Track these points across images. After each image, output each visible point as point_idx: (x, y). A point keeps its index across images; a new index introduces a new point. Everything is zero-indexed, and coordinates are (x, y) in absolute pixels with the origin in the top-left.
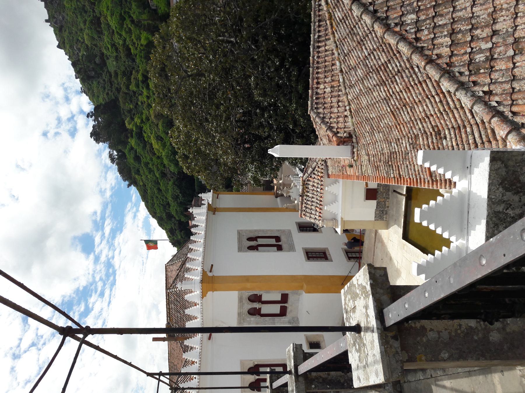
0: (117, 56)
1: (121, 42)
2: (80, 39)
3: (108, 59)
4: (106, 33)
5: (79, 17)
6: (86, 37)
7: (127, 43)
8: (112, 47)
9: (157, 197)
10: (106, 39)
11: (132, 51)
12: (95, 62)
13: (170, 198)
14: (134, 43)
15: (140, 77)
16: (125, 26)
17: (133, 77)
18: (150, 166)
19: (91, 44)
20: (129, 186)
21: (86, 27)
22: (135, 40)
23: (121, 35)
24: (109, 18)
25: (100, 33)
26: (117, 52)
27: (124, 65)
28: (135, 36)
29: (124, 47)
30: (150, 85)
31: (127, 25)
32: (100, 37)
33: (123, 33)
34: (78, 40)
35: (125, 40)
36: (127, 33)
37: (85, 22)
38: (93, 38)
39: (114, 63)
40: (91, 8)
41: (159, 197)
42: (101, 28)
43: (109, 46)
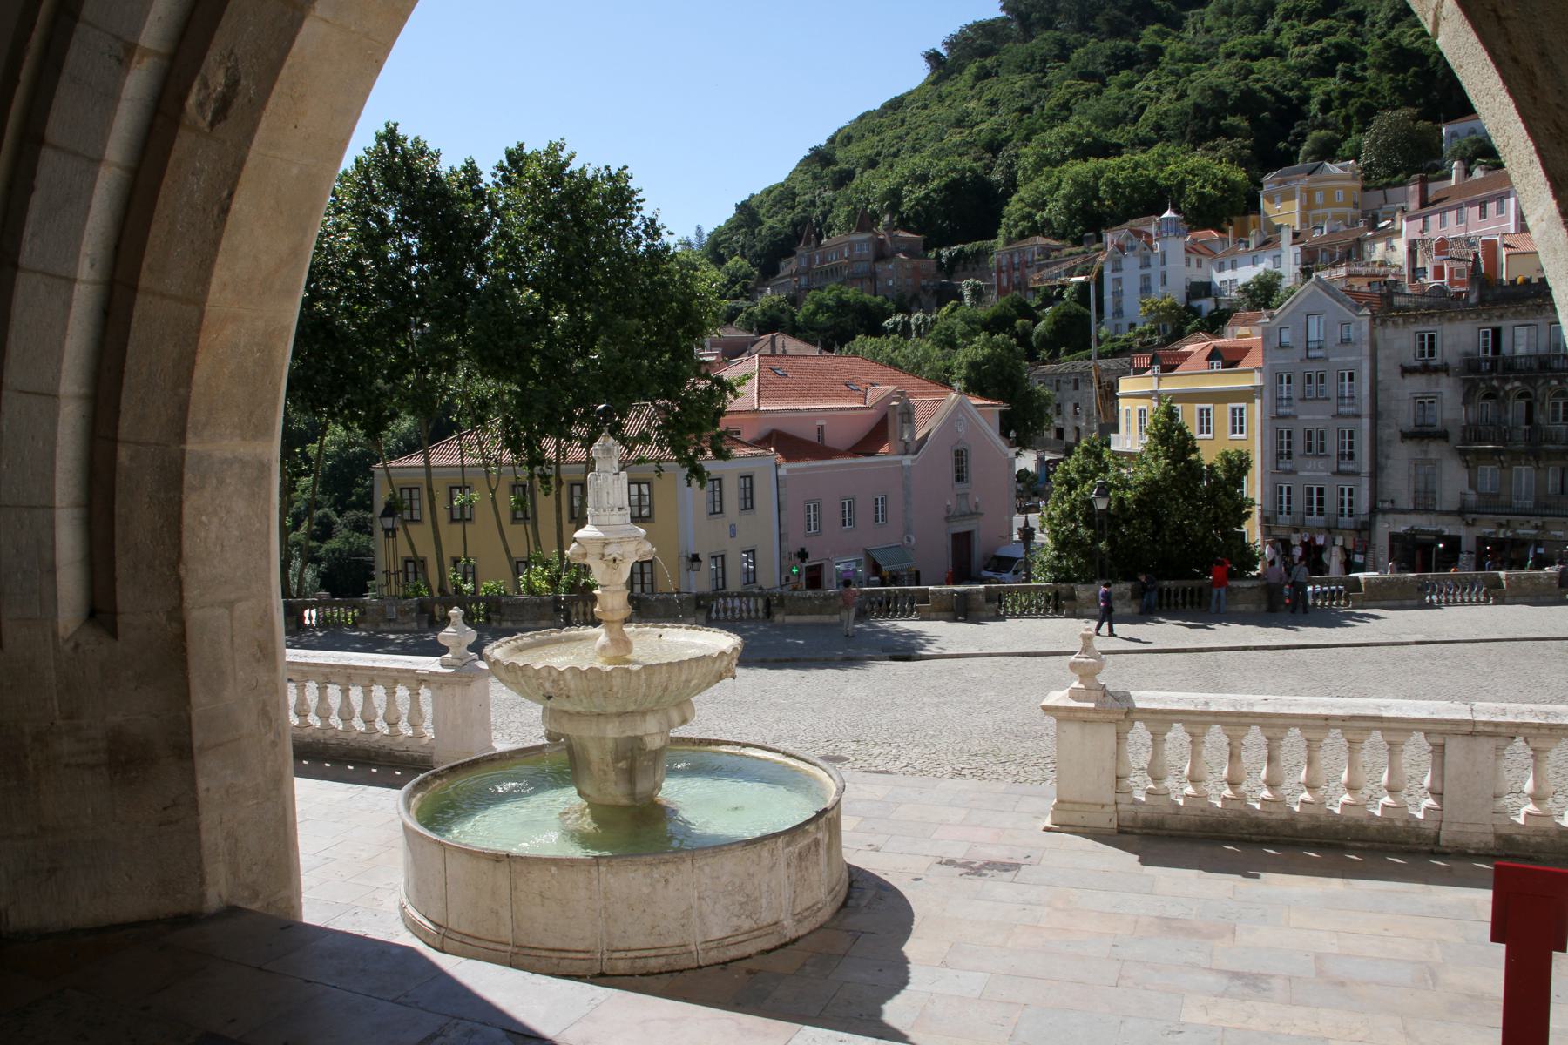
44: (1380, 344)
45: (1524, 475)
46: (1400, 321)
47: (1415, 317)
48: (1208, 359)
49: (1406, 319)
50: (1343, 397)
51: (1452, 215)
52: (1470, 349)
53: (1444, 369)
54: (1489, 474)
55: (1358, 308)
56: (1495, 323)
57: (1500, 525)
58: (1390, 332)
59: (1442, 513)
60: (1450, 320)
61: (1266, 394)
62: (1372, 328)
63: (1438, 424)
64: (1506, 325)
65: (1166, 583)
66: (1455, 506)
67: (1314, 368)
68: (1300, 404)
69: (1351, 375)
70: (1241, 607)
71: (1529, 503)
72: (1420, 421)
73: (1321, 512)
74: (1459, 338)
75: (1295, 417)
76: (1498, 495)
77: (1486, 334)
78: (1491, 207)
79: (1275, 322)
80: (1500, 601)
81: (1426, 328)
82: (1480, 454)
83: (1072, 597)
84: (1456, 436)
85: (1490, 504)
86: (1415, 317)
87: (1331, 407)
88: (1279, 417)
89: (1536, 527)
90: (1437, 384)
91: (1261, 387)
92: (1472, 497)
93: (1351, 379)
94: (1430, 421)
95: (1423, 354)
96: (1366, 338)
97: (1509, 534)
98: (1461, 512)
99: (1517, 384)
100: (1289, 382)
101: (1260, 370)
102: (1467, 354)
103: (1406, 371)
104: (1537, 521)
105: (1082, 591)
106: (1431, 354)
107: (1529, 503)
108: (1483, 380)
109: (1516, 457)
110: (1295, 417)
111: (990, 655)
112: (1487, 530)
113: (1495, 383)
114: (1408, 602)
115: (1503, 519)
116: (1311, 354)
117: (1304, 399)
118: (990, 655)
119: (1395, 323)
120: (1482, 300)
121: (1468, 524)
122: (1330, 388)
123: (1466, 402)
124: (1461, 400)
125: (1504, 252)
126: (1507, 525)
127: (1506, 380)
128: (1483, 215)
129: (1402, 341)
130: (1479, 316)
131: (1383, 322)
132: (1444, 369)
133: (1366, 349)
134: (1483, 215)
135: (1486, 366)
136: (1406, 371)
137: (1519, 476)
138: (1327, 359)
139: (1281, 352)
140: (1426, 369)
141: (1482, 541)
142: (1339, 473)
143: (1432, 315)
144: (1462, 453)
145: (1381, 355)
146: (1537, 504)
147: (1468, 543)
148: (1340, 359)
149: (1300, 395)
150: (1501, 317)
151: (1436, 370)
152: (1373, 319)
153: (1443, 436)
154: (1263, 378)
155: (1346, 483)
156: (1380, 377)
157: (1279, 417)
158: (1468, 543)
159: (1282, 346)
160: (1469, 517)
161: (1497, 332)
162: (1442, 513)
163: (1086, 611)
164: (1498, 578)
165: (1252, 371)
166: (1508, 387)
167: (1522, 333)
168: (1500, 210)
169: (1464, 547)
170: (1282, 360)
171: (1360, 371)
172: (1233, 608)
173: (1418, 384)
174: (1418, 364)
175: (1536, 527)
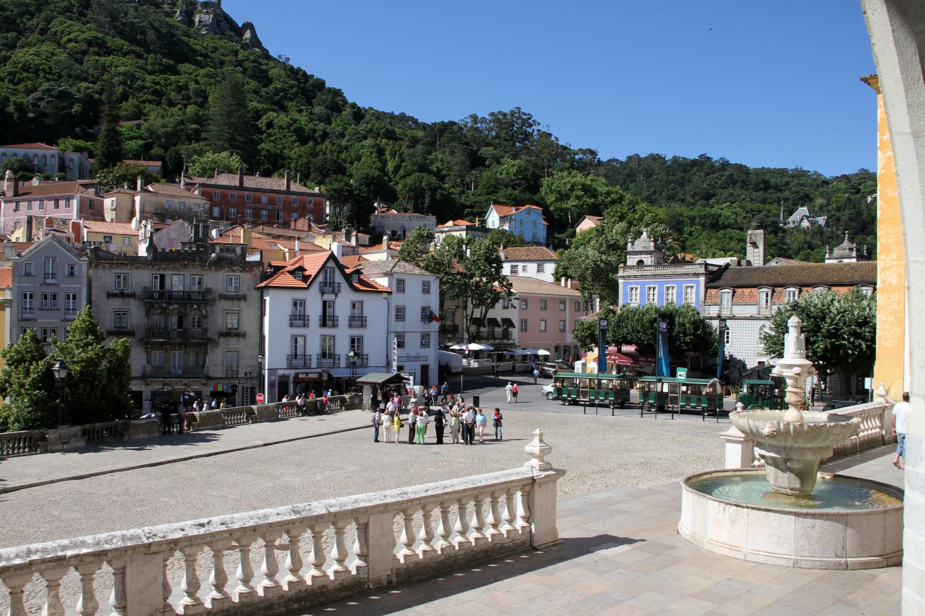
44: (94, 279)
45: (177, 357)
46: (107, 266)
47: (116, 264)
49: (111, 265)
50: (69, 309)
51: (36, 204)
52: (148, 285)
54: (157, 355)
55: (80, 256)
56: (162, 272)
57: (166, 384)
58: (100, 272)
60: (137, 268)
61: (15, 305)
62: (88, 268)
63: (129, 327)
64: (168, 273)
65: (97, 424)
66: (139, 374)
67: (50, 291)
68: (40, 312)
70: (141, 436)
71: (180, 372)
72: (117, 325)
74: (141, 279)
75: (36, 320)
76: (163, 367)
77: (156, 278)
78: (62, 203)
79: (23, 259)
80: (255, 422)
81: (123, 271)
82: (154, 344)
83: (43, 438)
84: (140, 334)
85: (159, 372)
86: (116, 264)
87: (61, 315)
88: (24, 320)
89: (185, 384)
90: (128, 304)
91: (11, 301)
92: (149, 369)
94: (124, 325)
95: (119, 286)
96: (84, 274)
97: (170, 388)
98: (144, 377)
99: (176, 306)
100: (31, 297)
101: (11, 289)
102: (145, 288)
103: (110, 295)
104: (185, 381)
105: (51, 434)
106: (125, 285)
107: (180, 372)
108: (157, 303)
109: (173, 346)
110: (36, 320)
111: (52, 482)
112: (157, 387)
113: (164, 305)
114: (218, 426)
115: (168, 380)
116: (48, 281)
117: (42, 309)
118: (52, 482)
119: (104, 268)
120: (155, 259)
121: (147, 384)
122: (61, 302)
123: (147, 316)
124: (144, 313)
125: (85, 231)
126: (169, 385)
127: (170, 304)
128: (57, 206)
129: (107, 278)
130: (153, 267)
131: (97, 266)
132: (133, 295)
133: (85, 281)
134: (57, 206)
135: (156, 295)
136: (110, 295)
137: (174, 357)
138: (58, 285)
139: (26, 279)
140: (122, 295)
141: (154, 394)
143: (127, 265)
144: (146, 344)
145: (93, 285)
146: (183, 372)
147: (146, 395)
148: (68, 286)
149: (39, 306)
150: (165, 269)
151: (129, 296)
152: (90, 264)
153: (131, 334)
154: (12, 295)
157: (24, 320)
158: (146, 395)
159: (28, 275)
160: (149, 380)
161: (162, 277)
163: (54, 448)
164: (252, 410)
165: (4, 290)
166: (171, 308)
167: (175, 278)
168: (68, 205)
169: (144, 397)
170: (28, 285)
171: (80, 294)
172: (137, 437)
173: (117, 303)
174: (117, 291)
175: (185, 384)
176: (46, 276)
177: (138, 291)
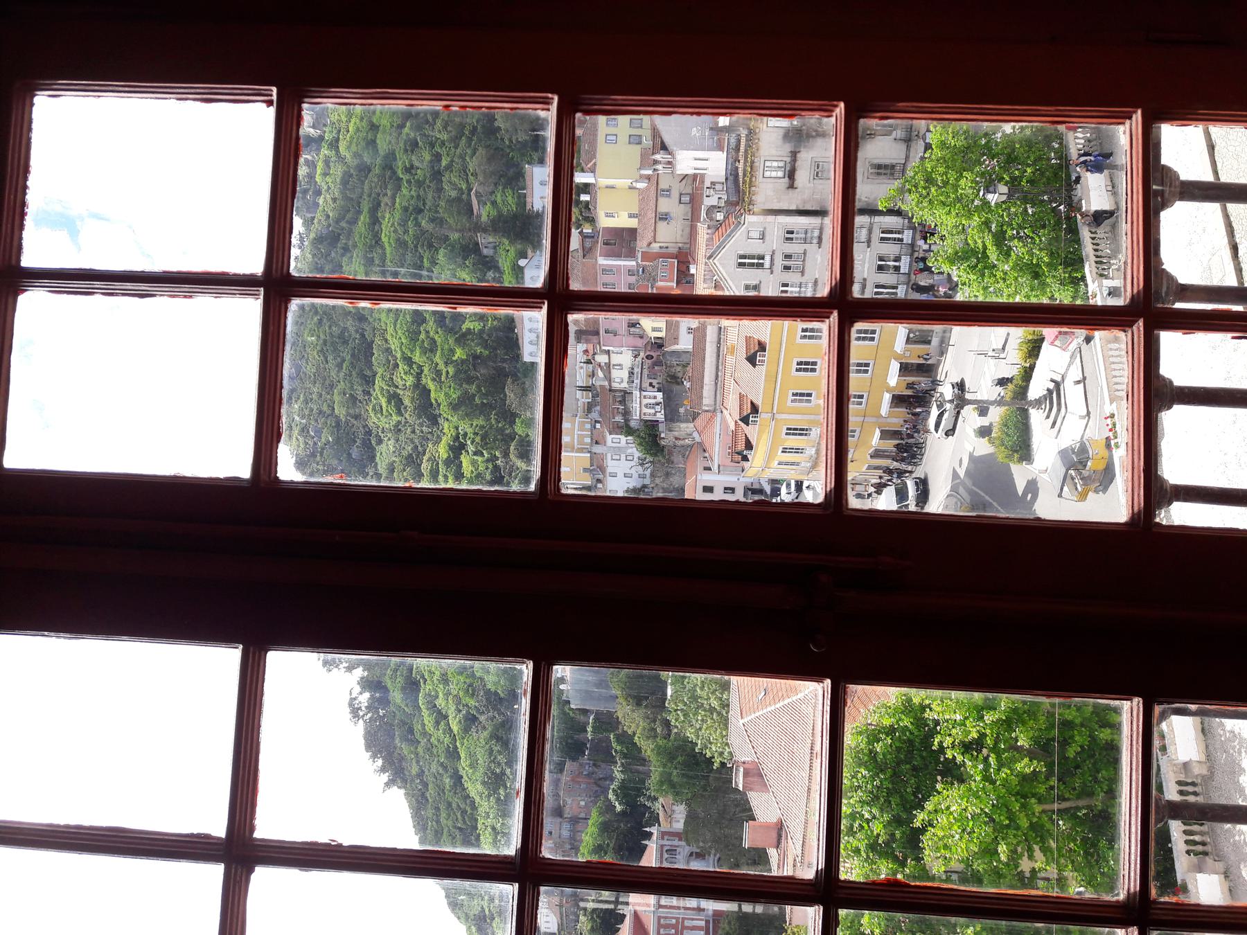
0: (399, 422)
1: (410, 380)
2: (325, 408)
3: (380, 442)
4: (380, 371)
5: (330, 358)
6: (337, 398)
7: (424, 381)
8: (389, 402)
9: (449, 805)
10: (379, 382)
11: (433, 395)
12: (349, 455)
13: (480, 787)
14: (439, 373)
15: (443, 451)
16: (423, 336)
17: (425, 458)
18: (441, 702)
19: (348, 414)
20: (388, 784)
21: (342, 375)
22: (441, 366)
23: (409, 361)
24: (390, 330)
25: (369, 381)
26: (399, 413)
27: (412, 441)
28: (442, 353)
29: (413, 392)
30: (464, 464)
31: (428, 332)
32: (369, 393)
33: (417, 357)
34: (321, 412)
35: (419, 376)
36: (424, 351)
37: (340, 366)
38: (353, 399)
39: (392, 442)
40: (357, 331)
41: (454, 805)
42: (370, 365)
43: (383, 401)
48: (754, 365)
52: (781, 132)
53: (794, 155)
59: (907, 158)
66: (903, 147)
67: (779, 262)
69: (788, 232)
73: (897, 259)
87: (812, 248)
93: (792, 232)
103: (792, 186)
116: (767, 265)
117: (803, 273)
132: (794, 155)
136: (792, 186)
142: (869, 242)
155: (877, 234)
156: (793, 207)
162: (907, 158)
173: (802, 177)
176: (760, 266)
177: (788, 148)
